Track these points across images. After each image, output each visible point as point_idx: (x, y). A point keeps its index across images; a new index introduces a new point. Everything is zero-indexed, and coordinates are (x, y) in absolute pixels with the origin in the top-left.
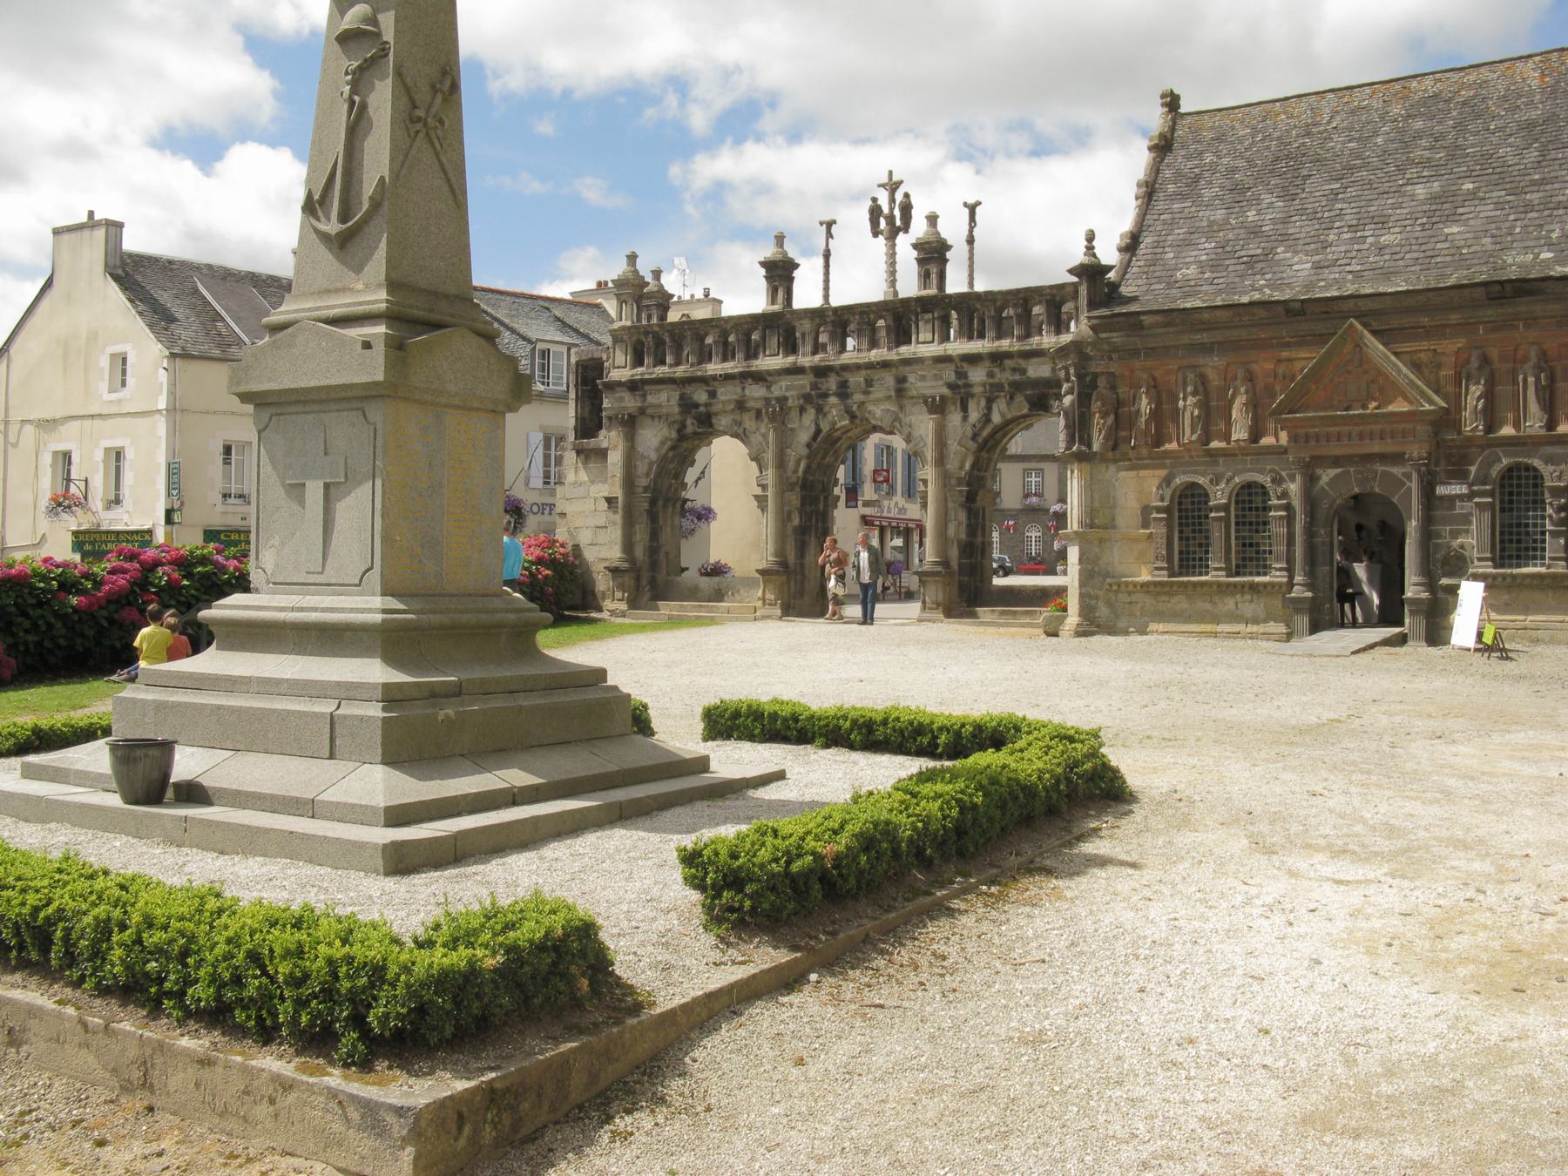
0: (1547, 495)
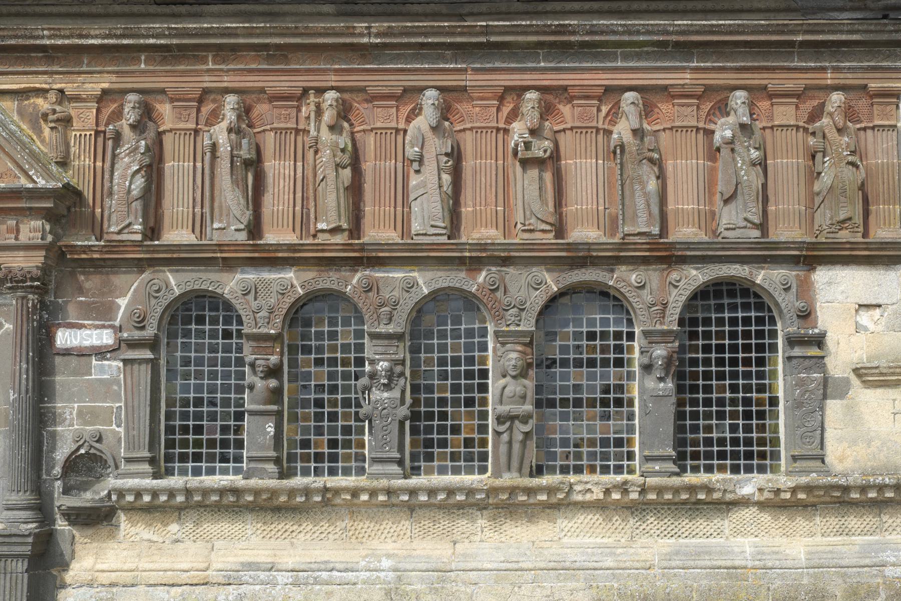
0: (247, 347)
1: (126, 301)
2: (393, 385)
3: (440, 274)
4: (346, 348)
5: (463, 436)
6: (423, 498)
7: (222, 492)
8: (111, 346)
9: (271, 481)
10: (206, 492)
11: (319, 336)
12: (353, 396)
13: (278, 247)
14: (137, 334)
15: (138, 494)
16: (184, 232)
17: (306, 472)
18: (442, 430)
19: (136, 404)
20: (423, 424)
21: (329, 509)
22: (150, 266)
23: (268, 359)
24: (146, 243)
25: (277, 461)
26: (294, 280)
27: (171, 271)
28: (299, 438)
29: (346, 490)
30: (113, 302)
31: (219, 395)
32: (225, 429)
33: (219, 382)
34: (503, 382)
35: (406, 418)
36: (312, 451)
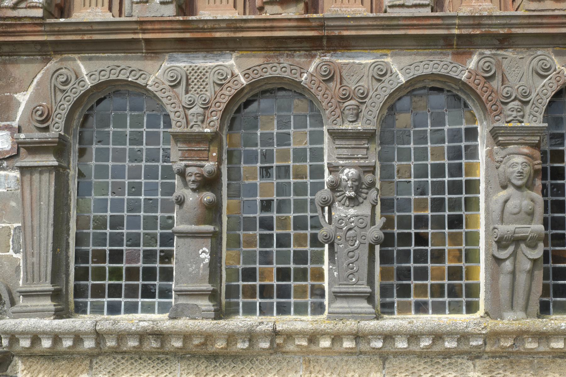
1: (27, 97)
2: (361, 200)
3: (419, 58)
4: (300, 155)
5: (447, 264)
6: (402, 344)
7: (142, 336)
8: (7, 152)
9: (205, 321)
10: (121, 336)
11: (267, 140)
12: (309, 214)
13: (215, 24)
14: (37, 136)
15: (36, 338)
16: (99, 10)
17: (249, 310)
18: (421, 257)
19: (36, 223)
20: (396, 249)
21: (279, 357)
22: (56, 52)
23: (202, 166)
24: (48, 21)
25: (214, 296)
26: (236, 68)
27: (82, 59)
28: (241, 266)
29: (301, 334)
30: (11, 98)
31: (142, 214)
32: (149, 256)
33: (142, 197)
34: (503, 194)
35: (377, 241)
36: (258, 283)
